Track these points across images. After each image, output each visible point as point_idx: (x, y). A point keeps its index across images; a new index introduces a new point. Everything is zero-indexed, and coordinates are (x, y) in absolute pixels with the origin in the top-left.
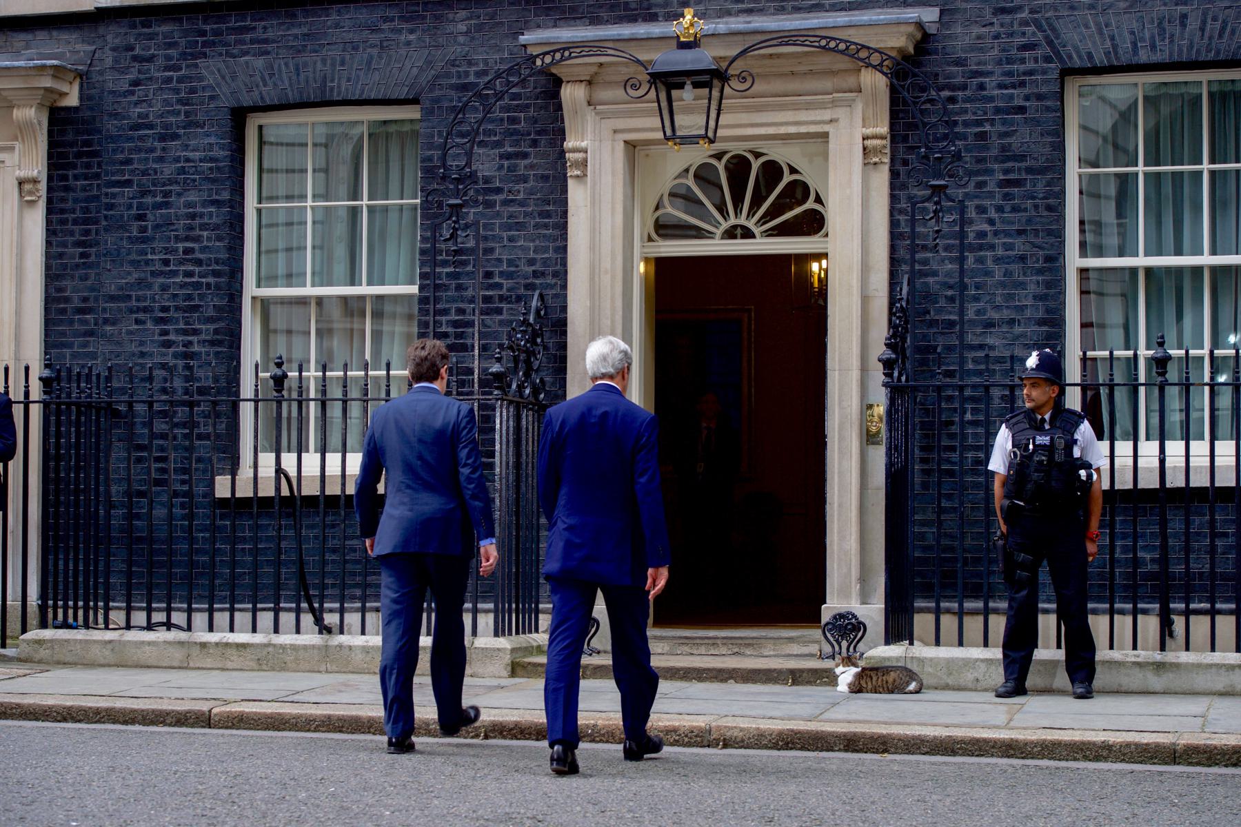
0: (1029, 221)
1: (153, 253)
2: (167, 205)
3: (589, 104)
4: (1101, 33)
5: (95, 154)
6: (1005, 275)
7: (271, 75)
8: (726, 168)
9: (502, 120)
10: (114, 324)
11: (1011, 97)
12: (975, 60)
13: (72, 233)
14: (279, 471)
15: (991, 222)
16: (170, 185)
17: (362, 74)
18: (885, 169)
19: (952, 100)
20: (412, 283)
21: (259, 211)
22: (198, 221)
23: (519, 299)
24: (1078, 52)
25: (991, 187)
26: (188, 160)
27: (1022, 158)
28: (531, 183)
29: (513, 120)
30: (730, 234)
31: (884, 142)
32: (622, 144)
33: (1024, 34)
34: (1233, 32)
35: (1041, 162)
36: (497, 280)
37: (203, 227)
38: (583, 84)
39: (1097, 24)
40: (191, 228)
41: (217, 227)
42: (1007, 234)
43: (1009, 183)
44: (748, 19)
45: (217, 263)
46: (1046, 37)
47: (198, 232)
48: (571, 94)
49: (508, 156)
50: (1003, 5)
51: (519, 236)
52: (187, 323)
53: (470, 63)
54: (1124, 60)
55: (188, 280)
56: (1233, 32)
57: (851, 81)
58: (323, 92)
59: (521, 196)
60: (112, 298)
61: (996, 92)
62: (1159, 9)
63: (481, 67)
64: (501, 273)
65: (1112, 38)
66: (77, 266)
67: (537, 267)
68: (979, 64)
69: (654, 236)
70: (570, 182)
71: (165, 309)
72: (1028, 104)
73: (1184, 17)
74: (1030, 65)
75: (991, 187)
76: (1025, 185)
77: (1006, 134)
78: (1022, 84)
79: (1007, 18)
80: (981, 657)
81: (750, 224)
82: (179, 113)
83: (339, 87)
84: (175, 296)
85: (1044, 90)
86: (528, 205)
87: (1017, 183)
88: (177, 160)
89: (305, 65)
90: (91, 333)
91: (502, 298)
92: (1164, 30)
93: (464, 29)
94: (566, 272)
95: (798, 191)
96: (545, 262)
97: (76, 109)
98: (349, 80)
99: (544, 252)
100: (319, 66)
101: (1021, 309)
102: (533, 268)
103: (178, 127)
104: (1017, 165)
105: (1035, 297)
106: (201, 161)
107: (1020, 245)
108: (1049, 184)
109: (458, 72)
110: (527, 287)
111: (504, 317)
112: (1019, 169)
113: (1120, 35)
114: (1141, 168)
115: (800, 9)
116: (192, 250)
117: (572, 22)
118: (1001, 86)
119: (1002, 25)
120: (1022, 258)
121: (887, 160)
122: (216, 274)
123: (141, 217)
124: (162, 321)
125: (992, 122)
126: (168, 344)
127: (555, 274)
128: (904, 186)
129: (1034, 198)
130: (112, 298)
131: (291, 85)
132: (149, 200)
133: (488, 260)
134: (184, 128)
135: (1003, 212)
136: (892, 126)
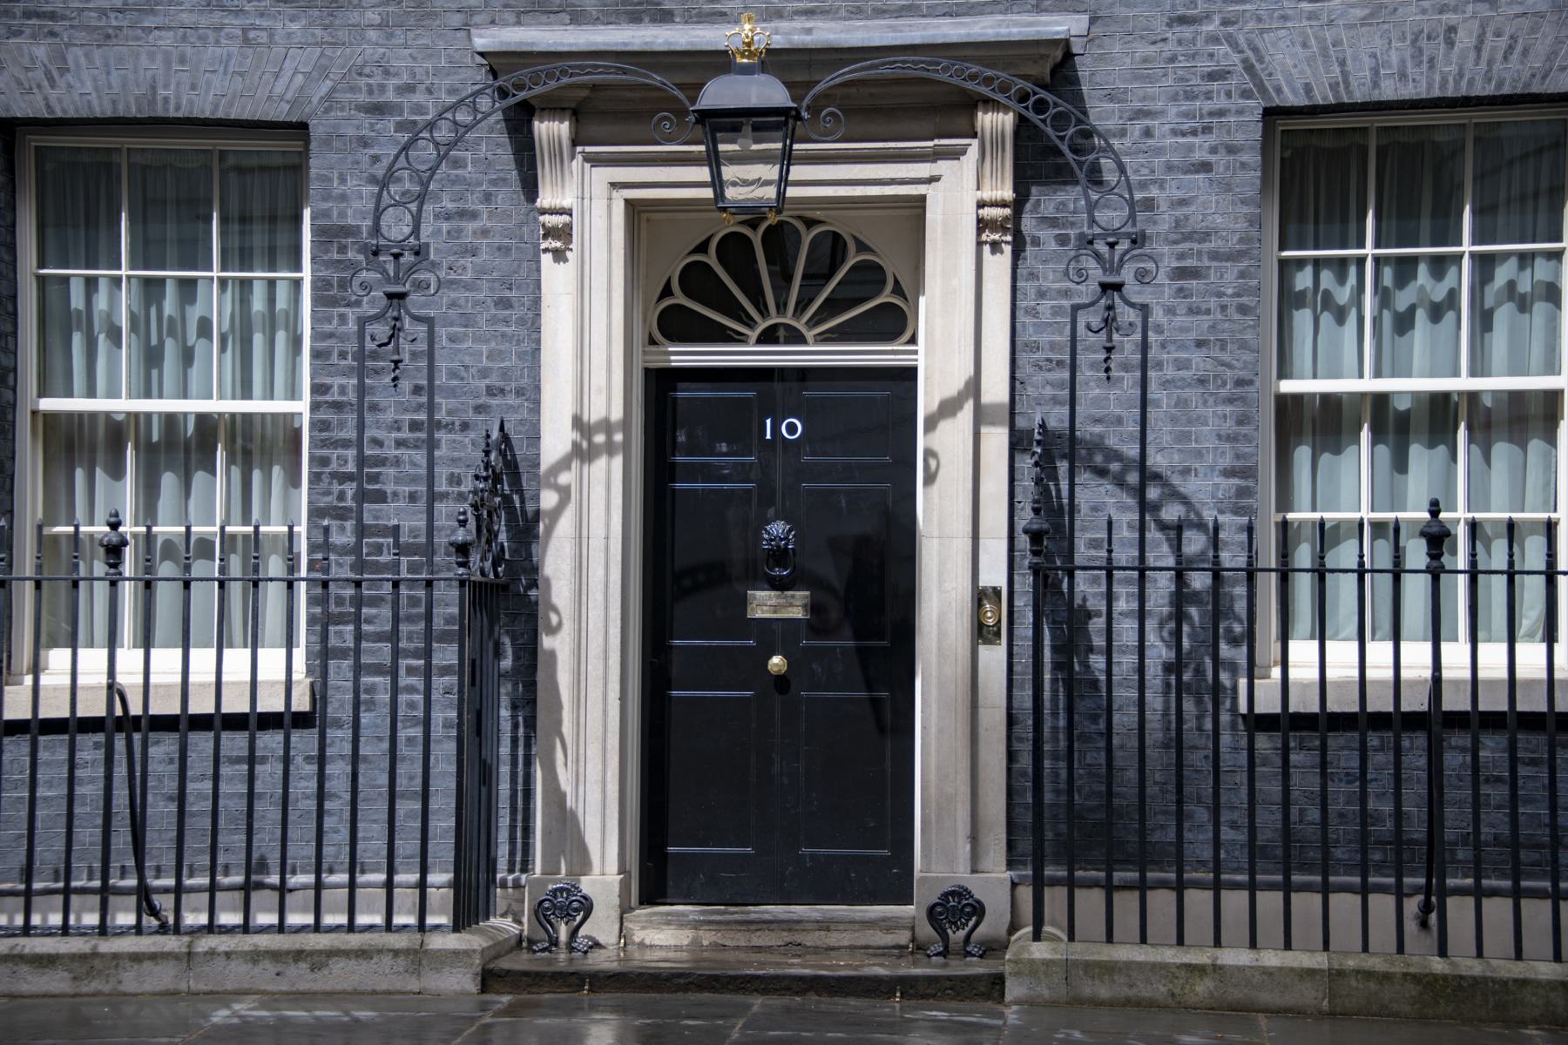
0: (1213, 327)
3: (575, 143)
4: (1326, 55)
6: (1176, 405)
7: (64, 71)
11: (1190, 148)
12: (1141, 93)
14: (113, 689)
17: (213, 77)
20: (293, 394)
21: (42, 281)
23: (465, 426)
24: (1290, 83)
25: (1161, 278)
27: (1206, 236)
28: (484, 256)
30: (768, 337)
31: (1007, 211)
32: (622, 203)
33: (1211, 55)
34: (1525, 52)
35: (1233, 243)
38: (568, 113)
39: (1321, 41)
42: (1182, 346)
44: (809, 25)
46: (1245, 61)
48: (551, 130)
49: (448, 217)
50: (1181, 11)
51: (465, 335)
53: (387, 73)
54: (1359, 96)
56: (1525, 52)
57: (961, 122)
58: (153, 102)
61: (1169, 141)
62: (1412, 17)
63: (406, 78)
65: (1342, 63)
67: (494, 380)
68: (1144, 99)
69: (658, 336)
70: (547, 259)
72: (1213, 158)
73: (1452, 29)
74: (1220, 102)
75: (1161, 278)
76: (1207, 277)
77: (1183, 202)
78: (1207, 130)
79: (1186, 32)
80: (1178, 961)
81: (800, 325)
83: (178, 97)
85: (1239, 138)
86: (478, 289)
87: (1193, 273)
89: (120, 60)
92: (1420, 50)
93: (377, 19)
94: (538, 389)
95: (871, 276)
96: (505, 374)
98: (193, 87)
99: (503, 360)
100: (144, 61)
101: (1199, 454)
102: (487, 381)
104: (1196, 246)
105: (1219, 437)
107: (1199, 361)
108: (1242, 275)
109: (369, 85)
110: (478, 409)
112: (1200, 253)
113: (1355, 59)
114: (1369, 250)
115: (884, 12)
117: (544, 18)
118: (1174, 133)
119: (1180, 42)
120: (1202, 381)
121: (1009, 238)
125: (1162, 184)
127: (519, 392)
128: (1033, 276)
129: (1220, 295)
131: (96, 89)
135: (1175, 314)
136: (1015, 190)
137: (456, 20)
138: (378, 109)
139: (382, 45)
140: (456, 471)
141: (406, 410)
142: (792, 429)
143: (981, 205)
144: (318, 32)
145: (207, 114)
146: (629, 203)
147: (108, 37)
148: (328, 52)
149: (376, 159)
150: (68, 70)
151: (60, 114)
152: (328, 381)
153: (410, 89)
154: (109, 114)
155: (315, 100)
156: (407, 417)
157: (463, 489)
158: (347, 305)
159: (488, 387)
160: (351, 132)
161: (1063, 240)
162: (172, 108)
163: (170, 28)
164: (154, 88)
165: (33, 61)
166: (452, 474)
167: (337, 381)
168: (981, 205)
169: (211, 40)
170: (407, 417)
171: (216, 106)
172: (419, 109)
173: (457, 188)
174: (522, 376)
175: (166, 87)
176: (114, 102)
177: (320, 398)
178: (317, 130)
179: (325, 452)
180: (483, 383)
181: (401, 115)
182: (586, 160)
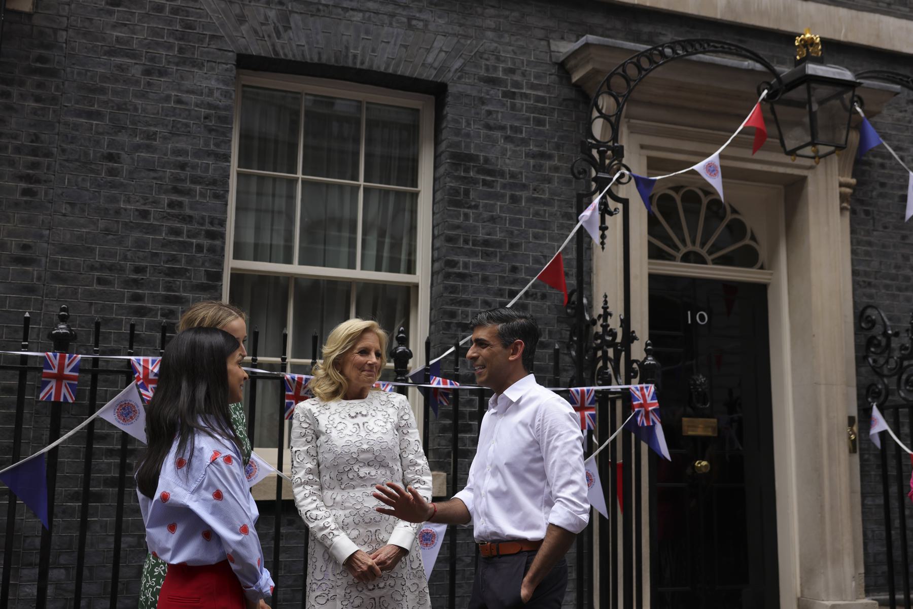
1: (128, 201)
2: (148, 148)
5: (53, 73)
7: (287, 28)
8: (683, 200)
9: (528, 119)
10: (63, 280)
13: (12, 163)
16: (155, 126)
18: (848, 214)
19: (882, 166)
22: (189, 172)
26: (179, 101)
29: (540, 122)
36: (523, 276)
37: (195, 180)
40: (177, 179)
41: (214, 182)
45: (212, 223)
47: (188, 185)
49: (534, 156)
52: (169, 288)
53: (498, 59)
55: (172, 238)
59: (546, 196)
60: (65, 250)
63: (510, 65)
64: (527, 268)
66: (17, 204)
71: (138, 270)
81: (703, 252)
82: (170, 47)
84: (156, 255)
88: (167, 98)
90: (31, 290)
93: (493, 25)
95: (737, 229)
97: (29, 15)
98: (373, 51)
103: (169, 62)
106: (197, 105)
109: (486, 65)
116: (180, 205)
122: (211, 235)
123: (111, 157)
124: (136, 283)
126: (141, 312)
130: (65, 250)
131: (308, 43)
132: (123, 138)
133: (515, 255)
134: (177, 64)
137: (540, 33)
138: (493, 82)
139: (496, 42)
141: (506, 283)
142: (702, 318)
143: (841, 185)
144: (457, 29)
145: (382, 69)
146: (650, 159)
147: (319, 10)
148: (462, 41)
149: (489, 113)
150: (290, 28)
151: (283, 57)
152: (456, 258)
153: (512, 71)
154: (316, 60)
155: (453, 70)
158: (468, 208)
160: (474, 93)
161: (867, 213)
162: (358, 62)
163: (361, 11)
164: (347, 48)
165: (266, 18)
167: (462, 259)
168: (841, 185)
169: (387, 21)
171: (388, 65)
172: (517, 85)
173: (540, 139)
175: (356, 48)
176: (319, 53)
177: (451, 270)
178: (452, 89)
179: (453, 307)
181: (506, 87)
182: (629, 127)
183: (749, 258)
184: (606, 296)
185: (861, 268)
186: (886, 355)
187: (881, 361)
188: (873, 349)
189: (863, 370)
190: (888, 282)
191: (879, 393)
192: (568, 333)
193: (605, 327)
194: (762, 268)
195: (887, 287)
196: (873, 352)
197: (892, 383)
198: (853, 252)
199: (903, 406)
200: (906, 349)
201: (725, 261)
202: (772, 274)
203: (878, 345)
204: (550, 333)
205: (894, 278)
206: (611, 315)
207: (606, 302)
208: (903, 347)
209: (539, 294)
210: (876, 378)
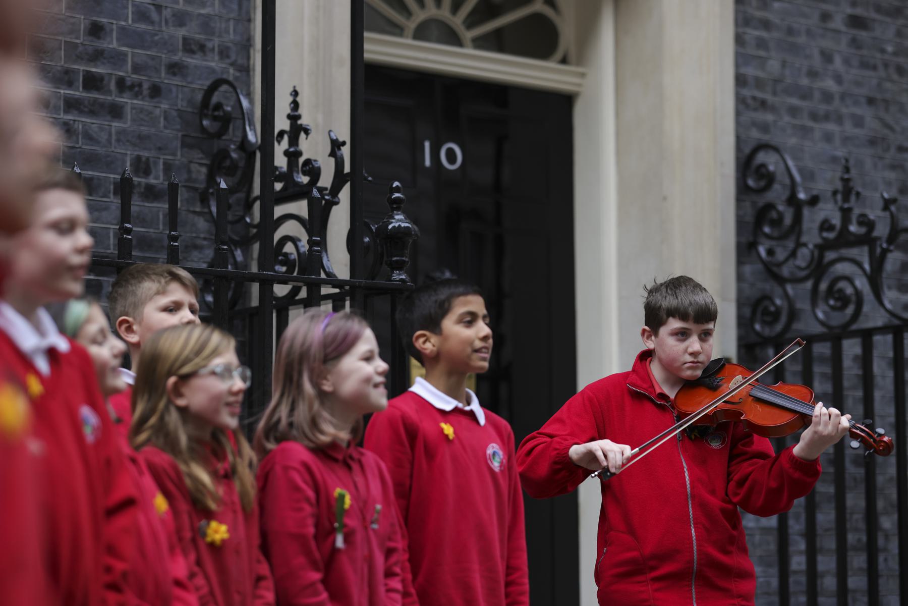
15: (839, 79)
23: (156, 91)
36: (115, 45)
43: (856, 22)
64: (122, 29)
67: (191, 31)
75: (838, 23)
81: (457, 22)
91: (121, 84)
96: (206, 24)
111: (126, 124)
120: (872, 142)
127: (224, 53)
140: (145, 154)
141: (79, 58)
156: (81, 67)
157: (152, 181)
159: (185, 39)
166: (139, 158)
170: (81, 67)
174: (228, 32)
180: (181, 32)
183: (539, 39)
184: (295, 93)
185: (750, 71)
186: (791, 244)
187: (781, 255)
188: (767, 230)
189: (747, 269)
190: (795, 101)
191: (776, 315)
192: (204, 170)
193: (293, 155)
194: (564, 61)
195: (793, 111)
196: (767, 236)
197: (799, 292)
198: (739, 40)
199: (820, 338)
200: (831, 228)
201: (497, 42)
202: (583, 75)
203: (777, 223)
204: (168, 167)
205: (806, 95)
206: (307, 131)
207: (295, 105)
208: (826, 226)
209: (146, 86)
210: (769, 286)
